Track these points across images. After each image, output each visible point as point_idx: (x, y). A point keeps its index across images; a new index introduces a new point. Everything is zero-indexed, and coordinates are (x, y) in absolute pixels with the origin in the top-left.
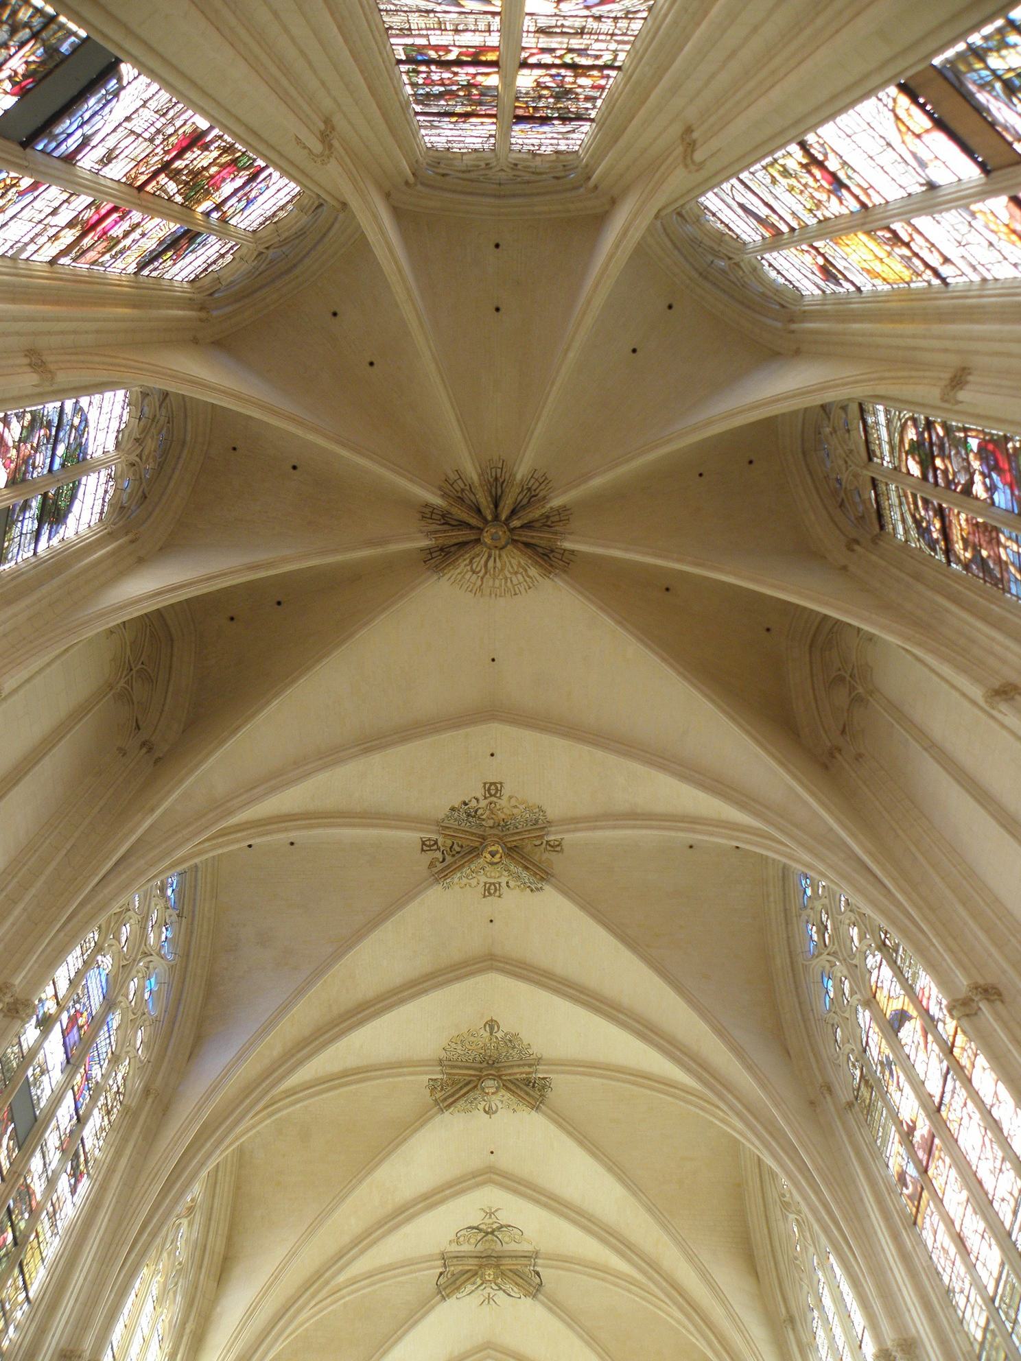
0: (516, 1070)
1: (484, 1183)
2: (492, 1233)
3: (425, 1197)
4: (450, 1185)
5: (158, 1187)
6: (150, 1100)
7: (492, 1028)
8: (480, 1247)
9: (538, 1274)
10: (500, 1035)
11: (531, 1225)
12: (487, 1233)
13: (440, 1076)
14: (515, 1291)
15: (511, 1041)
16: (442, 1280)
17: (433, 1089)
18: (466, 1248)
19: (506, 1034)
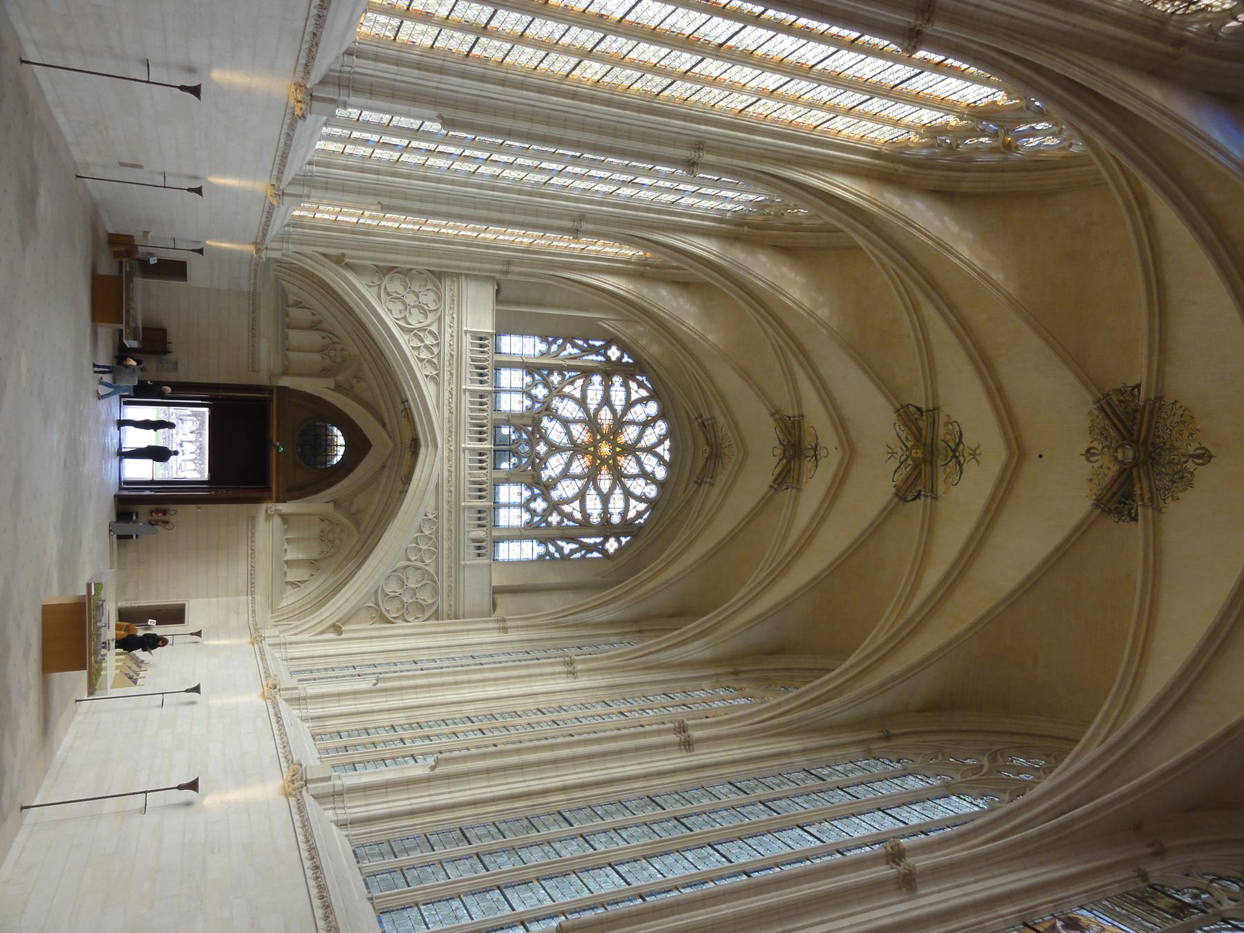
0: (1145, 483)
1: (1009, 448)
2: (955, 456)
3: (1000, 389)
4: (1009, 412)
5: (1077, 75)
6: (1170, 49)
7: (1198, 457)
8: (942, 444)
9: (917, 497)
10: (1190, 465)
11: (965, 495)
12: (954, 451)
13: (1142, 396)
14: (900, 477)
15: (1183, 479)
16: (912, 409)
17: (1120, 392)
18: (942, 431)
19: (1191, 473)
